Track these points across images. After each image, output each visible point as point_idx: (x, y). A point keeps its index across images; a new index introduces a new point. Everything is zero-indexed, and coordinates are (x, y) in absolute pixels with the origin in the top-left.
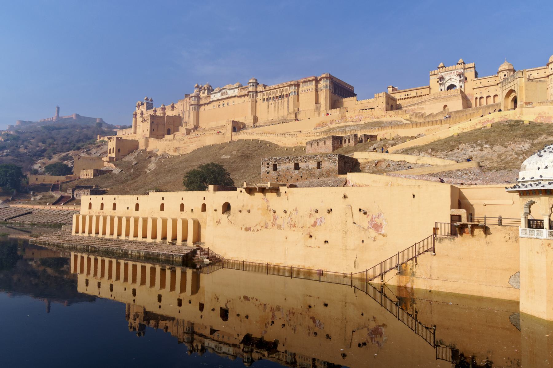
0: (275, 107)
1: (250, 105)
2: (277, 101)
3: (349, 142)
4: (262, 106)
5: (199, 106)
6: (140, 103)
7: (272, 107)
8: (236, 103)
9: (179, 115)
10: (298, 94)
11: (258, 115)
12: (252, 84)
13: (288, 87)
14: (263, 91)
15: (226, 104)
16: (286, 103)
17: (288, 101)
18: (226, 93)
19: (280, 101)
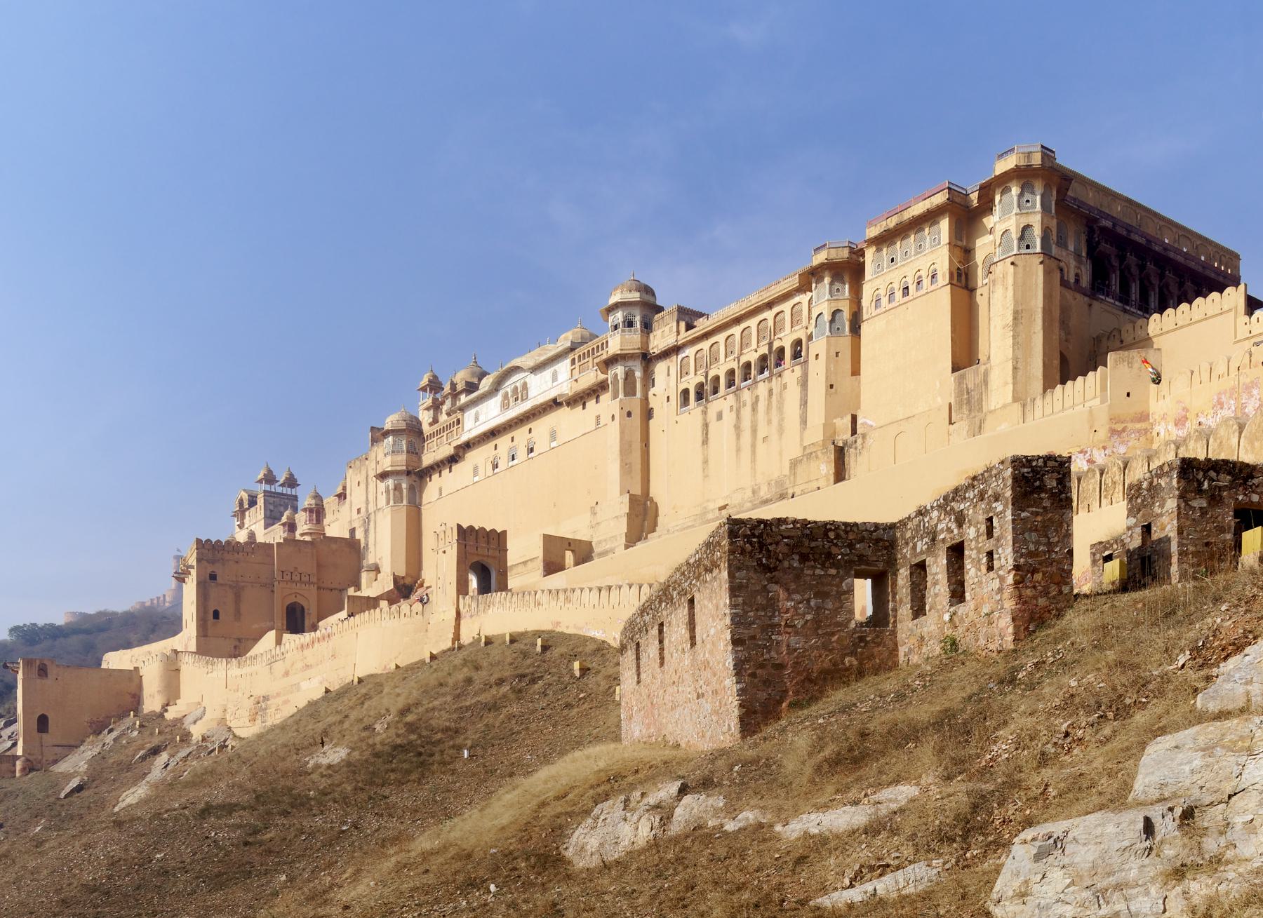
0: (737, 427)
1: (612, 433)
2: (746, 396)
3: (958, 595)
4: (674, 429)
5: (418, 475)
6: (245, 496)
7: (722, 432)
8: (563, 437)
9: (352, 531)
10: (856, 328)
11: (658, 491)
12: (619, 316)
13: (803, 298)
14: (676, 350)
15: (522, 454)
16: (793, 394)
17: (804, 382)
18: (521, 393)
19: (762, 389)
